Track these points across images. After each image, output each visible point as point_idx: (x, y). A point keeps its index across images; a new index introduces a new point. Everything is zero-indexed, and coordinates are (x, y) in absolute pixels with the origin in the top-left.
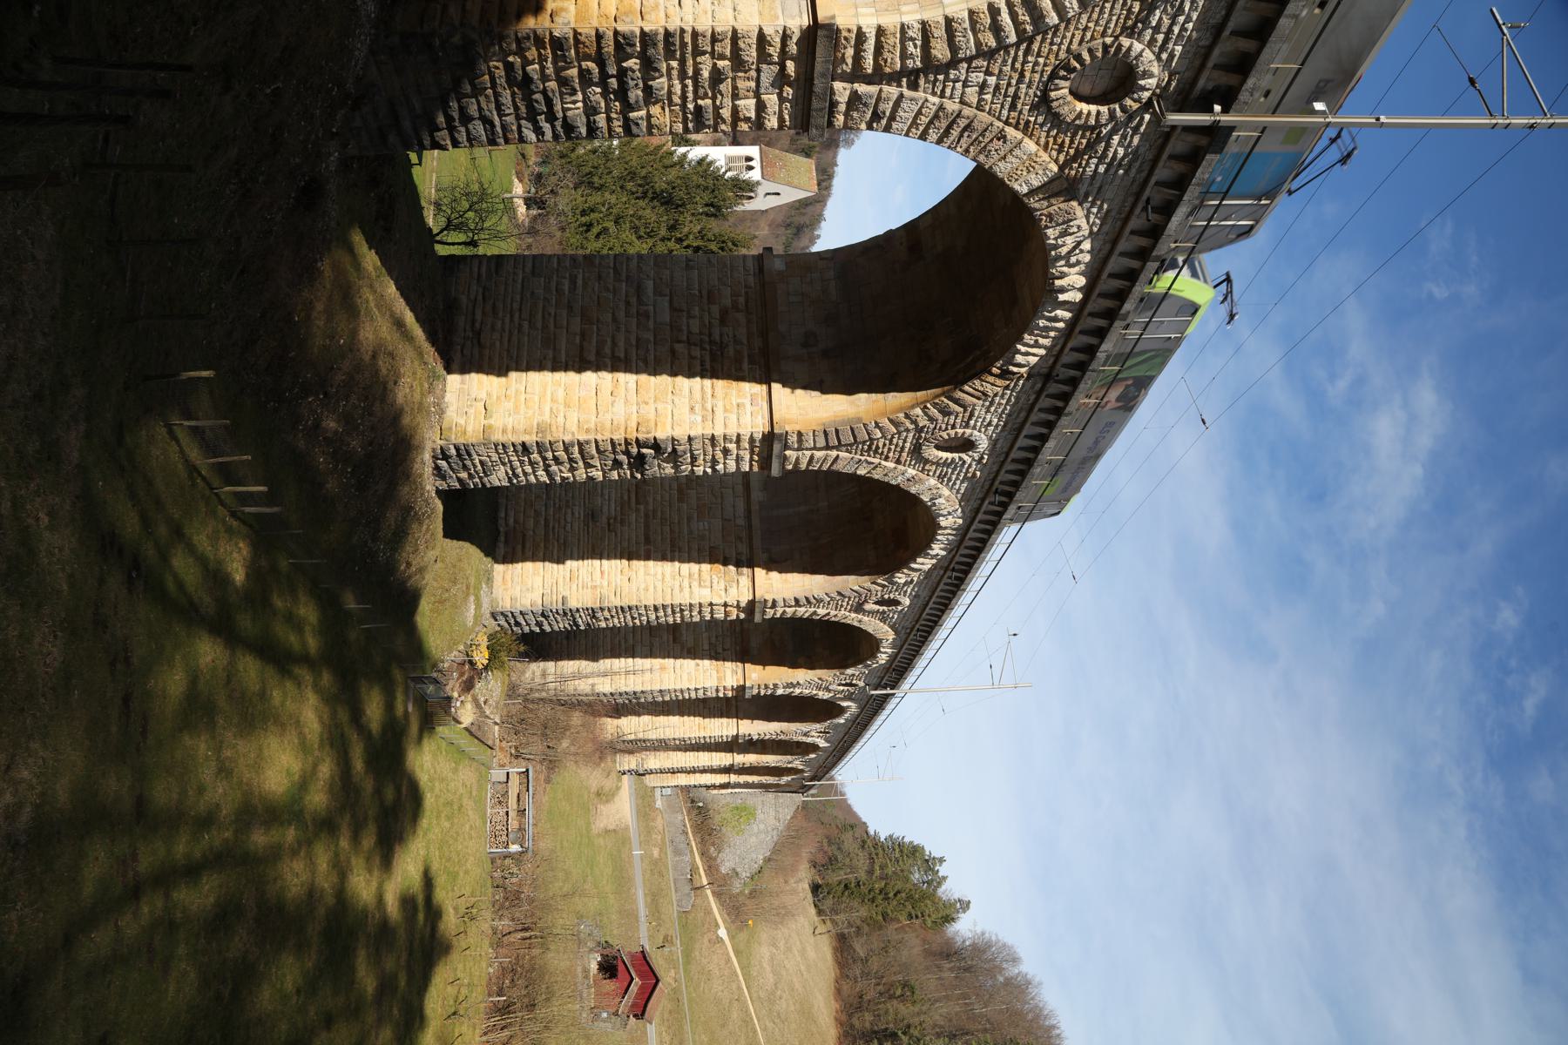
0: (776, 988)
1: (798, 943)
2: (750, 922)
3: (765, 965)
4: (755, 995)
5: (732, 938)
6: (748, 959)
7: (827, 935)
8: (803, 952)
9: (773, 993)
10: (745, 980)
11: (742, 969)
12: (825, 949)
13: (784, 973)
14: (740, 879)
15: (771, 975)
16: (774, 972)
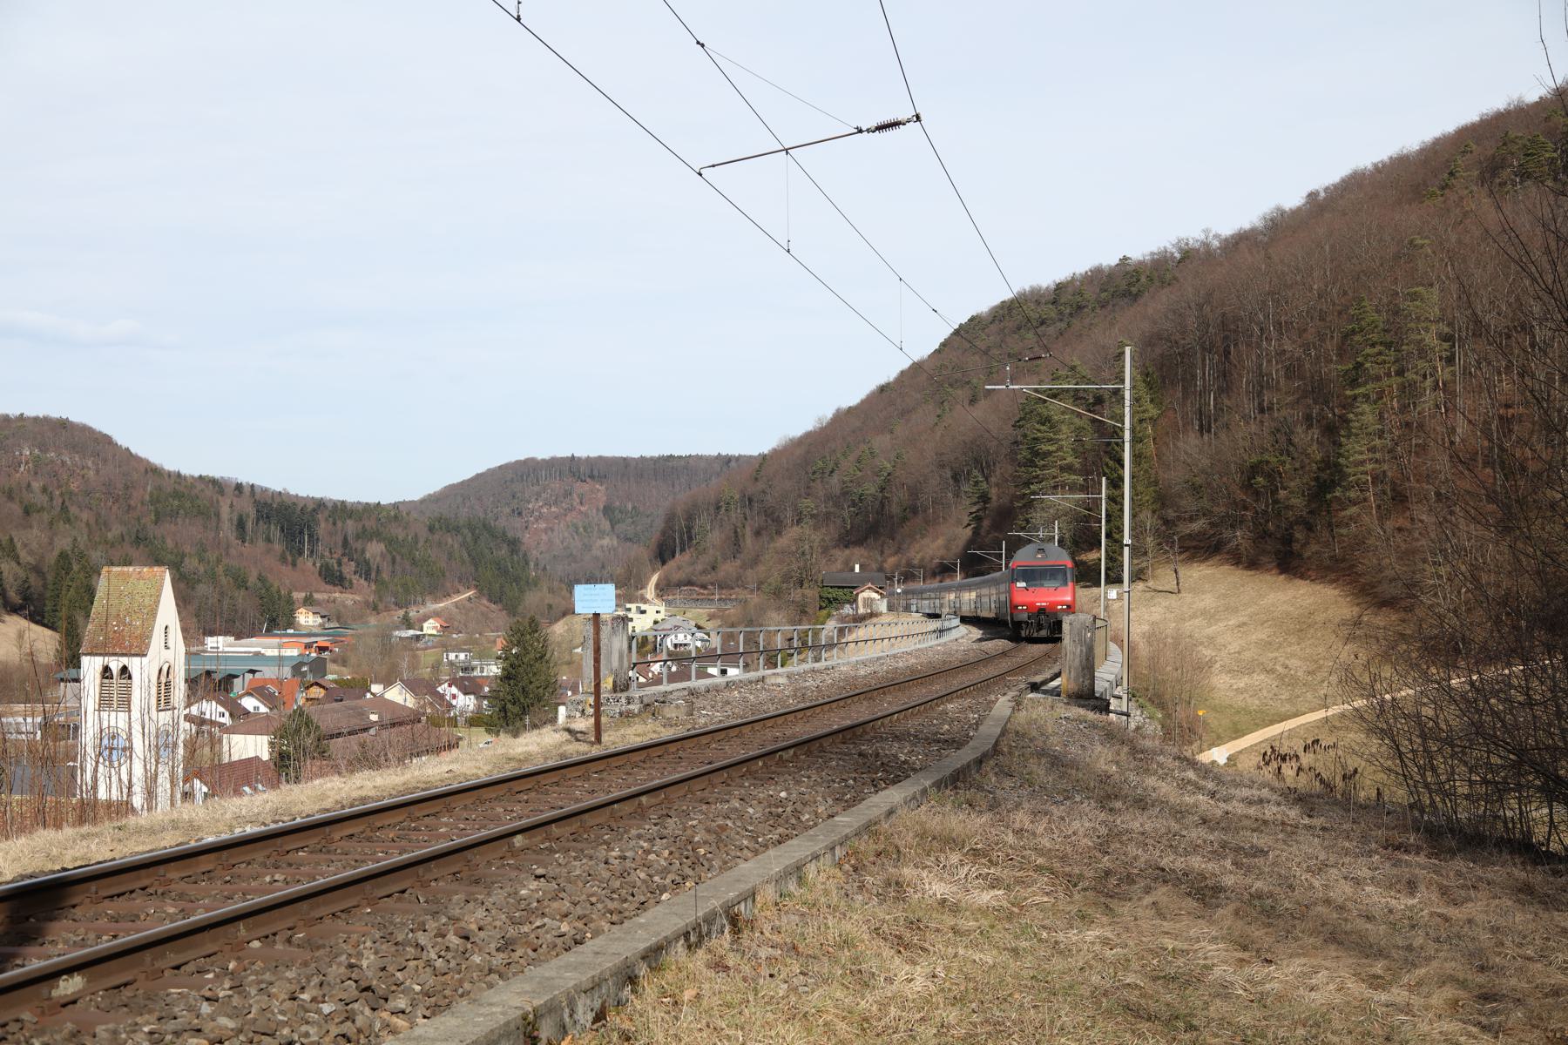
0: (1272, 671)
1: (1197, 622)
2: (1200, 713)
3: (1242, 685)
4: (1288, 707)
5: (1218, 741)
6: (1239, 712)
7: (1181, 574)
8: (1210, 616)
9: (1281, 678)
10: (1272, 723)
11: (1257, 726)
12: (1196, 575)
13: (1247, 655)
14: (1145, 723)
15: (1255, 675)
16: (1248, 669)
